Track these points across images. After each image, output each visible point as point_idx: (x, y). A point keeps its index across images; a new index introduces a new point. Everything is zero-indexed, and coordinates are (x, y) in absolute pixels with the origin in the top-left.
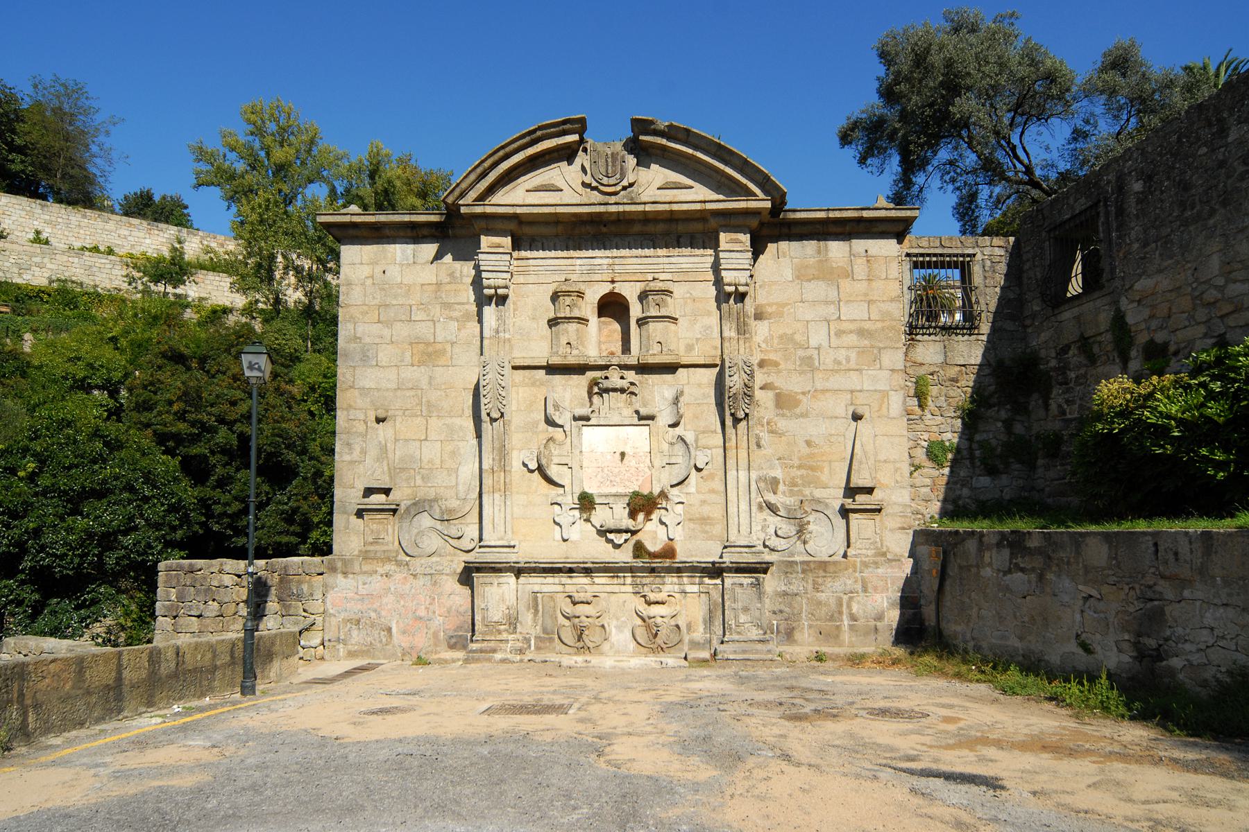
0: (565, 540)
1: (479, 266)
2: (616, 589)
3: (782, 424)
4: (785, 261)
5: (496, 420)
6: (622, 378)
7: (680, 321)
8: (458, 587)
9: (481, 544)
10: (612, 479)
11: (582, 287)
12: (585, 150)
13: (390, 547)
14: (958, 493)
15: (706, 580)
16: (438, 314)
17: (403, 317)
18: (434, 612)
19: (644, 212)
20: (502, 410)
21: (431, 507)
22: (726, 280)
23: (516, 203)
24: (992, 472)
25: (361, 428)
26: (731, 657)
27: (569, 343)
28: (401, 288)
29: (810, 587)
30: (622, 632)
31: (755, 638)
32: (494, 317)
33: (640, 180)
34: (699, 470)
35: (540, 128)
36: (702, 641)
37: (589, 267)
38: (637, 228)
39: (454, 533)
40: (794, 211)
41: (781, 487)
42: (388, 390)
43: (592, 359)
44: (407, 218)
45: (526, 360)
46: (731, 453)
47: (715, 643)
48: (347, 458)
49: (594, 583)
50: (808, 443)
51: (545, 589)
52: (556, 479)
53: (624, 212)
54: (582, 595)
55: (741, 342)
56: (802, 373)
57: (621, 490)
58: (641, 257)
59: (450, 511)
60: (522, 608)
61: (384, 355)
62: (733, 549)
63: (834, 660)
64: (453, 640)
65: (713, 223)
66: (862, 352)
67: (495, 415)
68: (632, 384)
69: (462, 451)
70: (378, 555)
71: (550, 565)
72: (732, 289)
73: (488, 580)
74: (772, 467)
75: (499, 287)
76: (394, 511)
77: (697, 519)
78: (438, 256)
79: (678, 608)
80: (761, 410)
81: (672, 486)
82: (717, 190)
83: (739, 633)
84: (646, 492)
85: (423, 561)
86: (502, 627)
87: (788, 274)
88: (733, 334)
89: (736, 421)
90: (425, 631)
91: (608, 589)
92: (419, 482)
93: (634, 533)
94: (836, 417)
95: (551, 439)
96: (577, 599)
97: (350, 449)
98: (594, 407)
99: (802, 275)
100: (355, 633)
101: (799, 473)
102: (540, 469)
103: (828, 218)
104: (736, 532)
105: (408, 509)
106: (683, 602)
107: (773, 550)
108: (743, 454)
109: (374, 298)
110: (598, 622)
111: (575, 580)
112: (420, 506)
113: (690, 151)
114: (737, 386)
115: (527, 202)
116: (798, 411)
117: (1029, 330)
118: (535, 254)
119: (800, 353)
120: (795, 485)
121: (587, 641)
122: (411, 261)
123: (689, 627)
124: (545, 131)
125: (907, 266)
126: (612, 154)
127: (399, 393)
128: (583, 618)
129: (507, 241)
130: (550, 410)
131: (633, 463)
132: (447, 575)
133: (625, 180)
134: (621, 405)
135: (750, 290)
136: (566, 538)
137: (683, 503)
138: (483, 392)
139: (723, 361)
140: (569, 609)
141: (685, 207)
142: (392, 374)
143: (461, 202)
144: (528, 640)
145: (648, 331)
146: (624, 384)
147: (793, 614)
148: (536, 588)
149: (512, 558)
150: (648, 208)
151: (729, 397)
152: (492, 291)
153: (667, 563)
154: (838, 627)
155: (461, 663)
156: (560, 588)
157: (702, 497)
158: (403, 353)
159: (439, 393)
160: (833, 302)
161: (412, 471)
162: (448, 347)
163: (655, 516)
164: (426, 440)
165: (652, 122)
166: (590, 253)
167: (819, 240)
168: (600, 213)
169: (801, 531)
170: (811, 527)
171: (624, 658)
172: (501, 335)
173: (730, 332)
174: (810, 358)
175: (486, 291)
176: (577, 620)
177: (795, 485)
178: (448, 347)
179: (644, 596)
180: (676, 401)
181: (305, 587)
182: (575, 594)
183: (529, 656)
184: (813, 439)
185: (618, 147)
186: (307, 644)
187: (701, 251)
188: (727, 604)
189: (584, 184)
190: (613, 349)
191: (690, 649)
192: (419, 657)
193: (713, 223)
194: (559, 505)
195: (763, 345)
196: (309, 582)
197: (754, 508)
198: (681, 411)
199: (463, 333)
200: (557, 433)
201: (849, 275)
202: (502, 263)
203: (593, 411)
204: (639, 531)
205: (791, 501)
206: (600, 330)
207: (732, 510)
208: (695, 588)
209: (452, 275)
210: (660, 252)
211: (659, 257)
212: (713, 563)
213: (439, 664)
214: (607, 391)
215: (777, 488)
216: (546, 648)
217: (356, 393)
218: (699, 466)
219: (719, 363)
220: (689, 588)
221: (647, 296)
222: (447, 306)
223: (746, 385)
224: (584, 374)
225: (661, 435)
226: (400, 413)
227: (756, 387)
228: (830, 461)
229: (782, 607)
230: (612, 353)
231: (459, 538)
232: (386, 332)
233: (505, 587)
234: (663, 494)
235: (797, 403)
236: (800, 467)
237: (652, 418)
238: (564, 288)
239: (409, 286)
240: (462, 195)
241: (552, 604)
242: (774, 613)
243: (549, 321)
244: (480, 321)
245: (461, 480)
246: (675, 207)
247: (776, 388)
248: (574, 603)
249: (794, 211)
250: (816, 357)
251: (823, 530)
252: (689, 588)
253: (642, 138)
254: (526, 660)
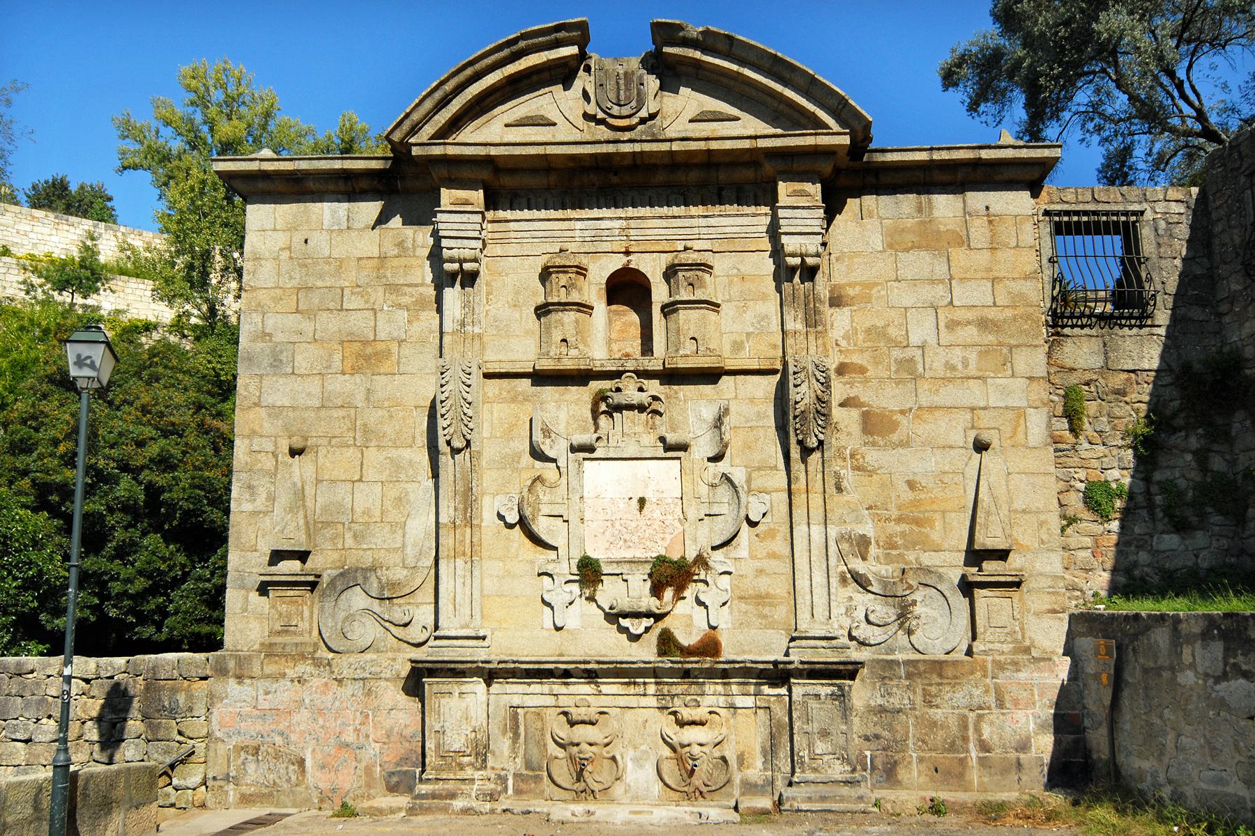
0: (558, 629)
1: (438, 230)
2: (633, 701)
3: (872, 457)
4: (871, 224)
5: (459, 451)
6: (641, 390)
7: (724, 307)
8: (402, 698)
9: (437, 633)
10: (627, 537)
11: (584, 261)
12: (588, 69)
13: (306, 638)
14: (1132, 558)
15: (766, 689)
16: (381, 300)
17: (332, 305)
18: (367, 736)
19: (671, 153)
20: (468, 437)
21: (366, 579)
22: (788, 249)
23: (489, 140)
24: (1181, 527)
25: (269, 463)
26: (804, 807)
27: (564, 340)
28: (329, 263)
29: (919, 699)
30: (641, 767)
31: (839, 777)
32: (458, 304)
33: (665, 110)
34: (753, 524)
35: (523, 37)
36: (760, 782)
37: (593, 233)
38: (660, 177)
39: (398, 615)
40: (884, 151)
41: (873, 550)
42: (307, 408)
43: (598, 363)
44: (337, 165)
45: (503, 365)
46: (799, 500)
47: (780, 784)
48: (248, 507)
49: (600, 693)
50: (911, 485)
51: (529, 701)
52: (544, 537)
53: (642, 153)
54: (583, 710)
55: (812, 338)
56: (899, 382)
57: (640, 554)
58: (667, 217)
59: (393, 585)
60: (495, 730)
62: (804, 643)
63: (957, 812)
64: (395, 779)
65: (768, 168)
66: (985, 352)
67: (458, 443)
68: (655, 398)
69: (412, 497)
70: (288, 649)
71: (536, 666)
72: (797, 261)
73: (445, 688)
74: (859, 521)
75: (466, 261)
76: (313, 586)
77: (751, 597)
78: (382, 219)
79: (724, 731)
80: (842, 436)
81: (714, 548)
82: (773, 120)
83: (815, 770)
84: (675, 556)
85: (351, 660)
86: (466, 759)
87: (877, 241)
88: (800, 326)
89: (806, 452)
90: (354, 764)
91: (622, 701)
92: (350, 542)
93: (659, 617)
94: (951, 447)
95: (538, 479)
96: (575, 717)
97: (253, 494)
98: (601, 433)
99: (895, 243)
100: (251, 767)
101: (899, 529)
102: (523, 523)
103: (932, 161)
104: (808, 616)
105: (332, 583)
106: (732, 721)
107: (863, 643)
108: (816, 500)
109: (291, 278)
110: (605, 752)
111: (572, 689)
112: (349, 578)
113: (734, 67)
114: (806, 401)
115: (506, 140)
116: (895, 437)
117: (1227, 319)
118: (518, 214)
119: (897, 353)
120: (893, 546)
121: (590, 781)
122: (344, 226)
123: (741, 760)
124: (530, 42)
125: (1046, 229)
126: (626, 74)
127: (323, 413)
128: (584, 746)
129: (478, 196)
130: (538, 436)
131: (657, 515)
132: (387, 680)
133: (645, 107)
134: (639, 429)
135: (823, 262)
136: (559, 624)
137: (729, 573)
138: (440, 410)
139: (785, 364)
140: (564, 732)
141: (728, 145)
142: (314, 386)
143: (412, 140)
144: (503, 780)
145: (677, 322)
146: (643, 398)
147: (895, 741)
148: (516, 701)
149: (481, 655)
150: (676, 147)
151: (795, 417)
152: (456, 266)
153: (707, 663)
154: (962, 762)
155: (403, 814)
156: (550, 701)
157: (758, 564)
158: (330, 355)
159: (380, 413)
160: (941, 281)
161: (340, 526)
162: (394, 347)
163: (689, 593)
164: (360, 480)
165: (680, 28)
166: (596, 213)
167: (919, 193)
168: (608, 154)
169: (904, 614)
170: (918, 610)
171: (645, 808)
172: (469, 328)
173: (795, 324)
174: (911, 360)
175: (448, 266)
176: (575, 749)
177: (893, 546)
178: (394, 347)
179: (674, 713)
180: (718, 423)
181: (181, 698)
182: (572, 710)
183: (504, 803)
184: (918, 479)
185: (634, 63)
186: (182, 783)
187: (752, 209)
188: (797, 725)
189: (587, 117)
190: (629, 350)
191: (743, 794)
192: (344, 805)
193: (768, 168)
194: (550, 575)
195: (843, 343)
196: (188, 690)
197: (834, 581)
198: (726, 438)
199: (416, 328)
200: (548, 470)
201: (963, 241)
202: (469, 227)
203: (598, 439)
204: (668, 613)
205: (887, 570)
206: (610, 322)
207: (802, 583)
208: (749, 701)
209: (400, 244)
210: (694, 210)
211: (692, 217)
212: (775, 663)
213: (371, 815)
214: (619, 408)
215: (867, 551)
216: (530, 791)
217: (263, 412)
218: (753, 518)
219: (779, 367)
220: (740, 701)
221: (676, 272)
222: (393, 288)
223: (818, 399)
224: (586, 384)
225: (697, 473)
226: (324, 441)
227: (834, 404)
228: (944, 512)
229: (879, 730)
230: (627, 355)
231: (406, 625)
232: (307, 326)
233: (469, 699)
234: (701, 561)
235: (894, 426)
236: (899, 520)
237: (684, 447)
238: (558, 261)
239: (341, 261)
240: (414, 130)
241: (539, 724)
242: (867, 739)
243: (537, 309)
244: (439, 310)
245: (410, 541)
246: (714, 145)
247: (862, 405)
248: (572, 724)
249: (884, 151)
250: (919, 359)
251: (935, 614)
252: (740, 701)
253: (666, 50)
254: (499, 810)
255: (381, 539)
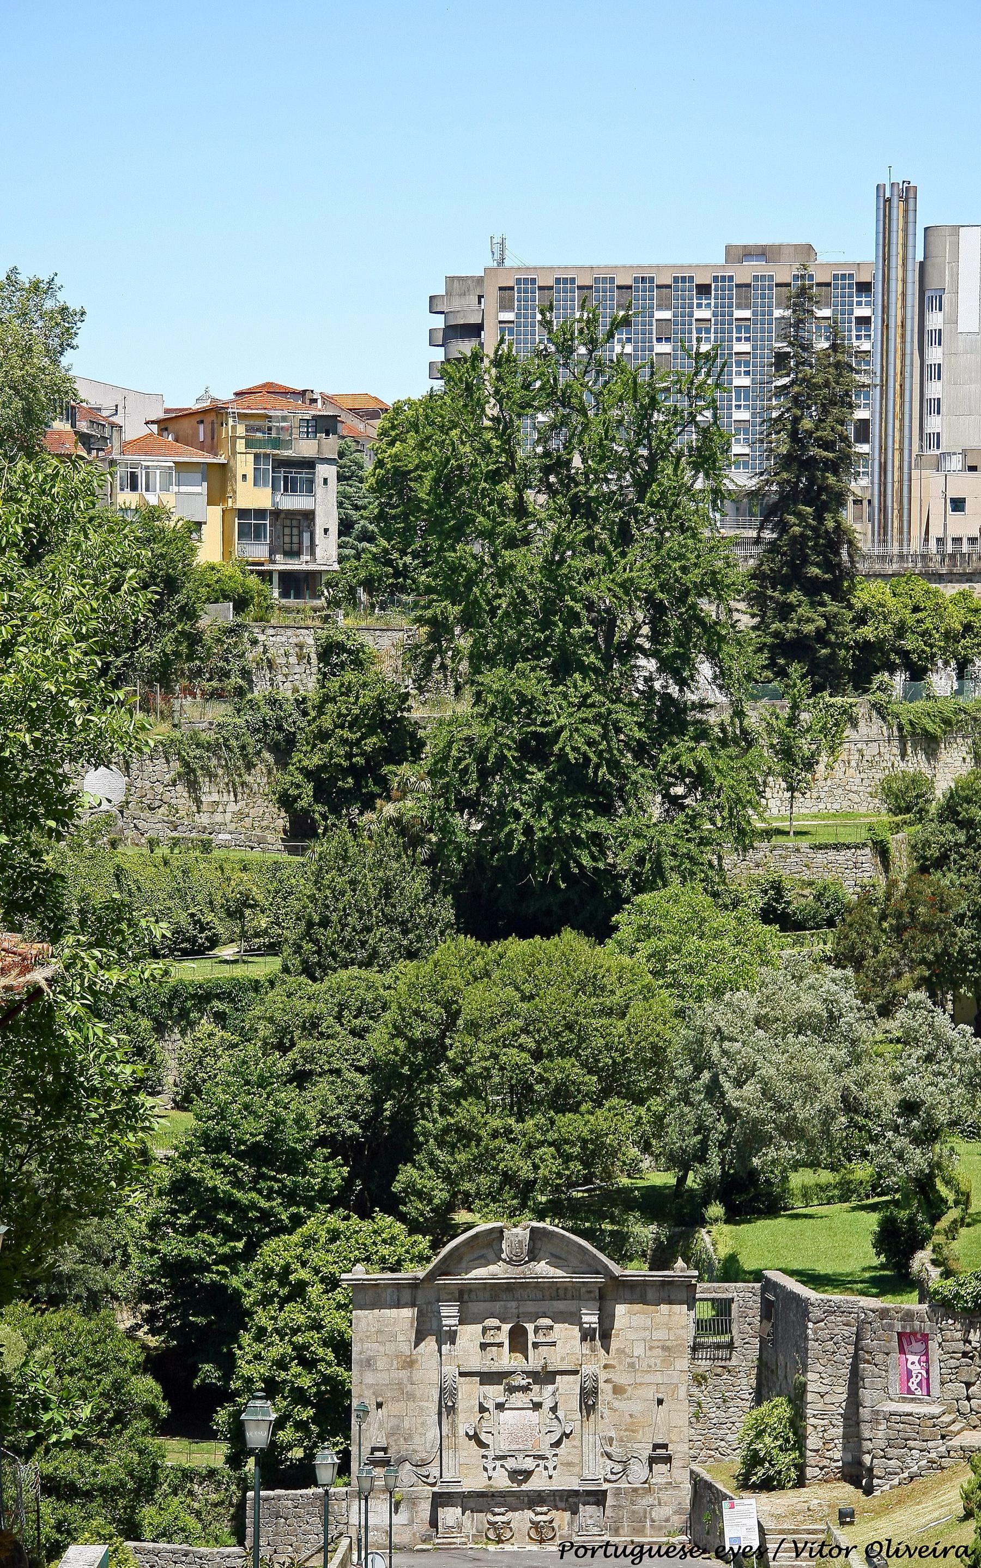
3: (616, 1404)
50: (631, 1416)
61: (381, 1364)
112: (402, 1461)
119: (628, 1360)
142: (385, 1375)
232: (382, 1349)
235: (625, 1391)
236: (626, 1430)
255: (417, 1439)
